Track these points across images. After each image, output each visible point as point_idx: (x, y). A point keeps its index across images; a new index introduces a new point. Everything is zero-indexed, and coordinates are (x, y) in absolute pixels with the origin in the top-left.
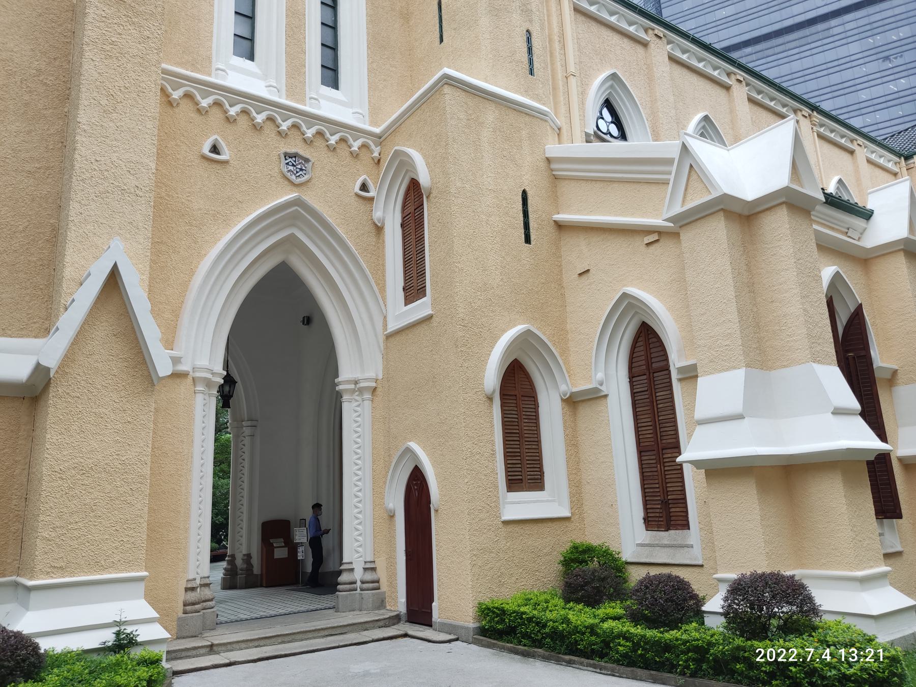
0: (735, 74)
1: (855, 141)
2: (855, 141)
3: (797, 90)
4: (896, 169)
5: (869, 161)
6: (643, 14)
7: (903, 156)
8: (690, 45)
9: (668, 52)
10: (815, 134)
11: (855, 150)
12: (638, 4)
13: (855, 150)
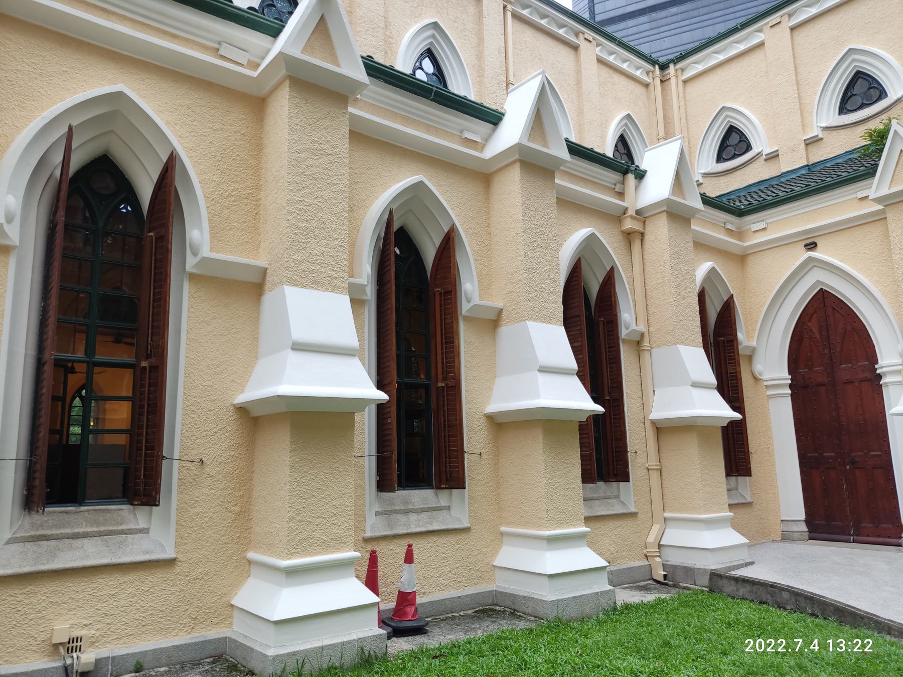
0: (583, 33)
1: (581, 34)
2: (581, 34)
3: (645, 49)
4: (646, 79)
5: (600, 61)
6: (556, 7)
7: (658, 64)
8: (579, 27)
9: (597, 54)
10: (509, 14)
11: (579, 45)
12: (578, 13)
13: (579, 45)
